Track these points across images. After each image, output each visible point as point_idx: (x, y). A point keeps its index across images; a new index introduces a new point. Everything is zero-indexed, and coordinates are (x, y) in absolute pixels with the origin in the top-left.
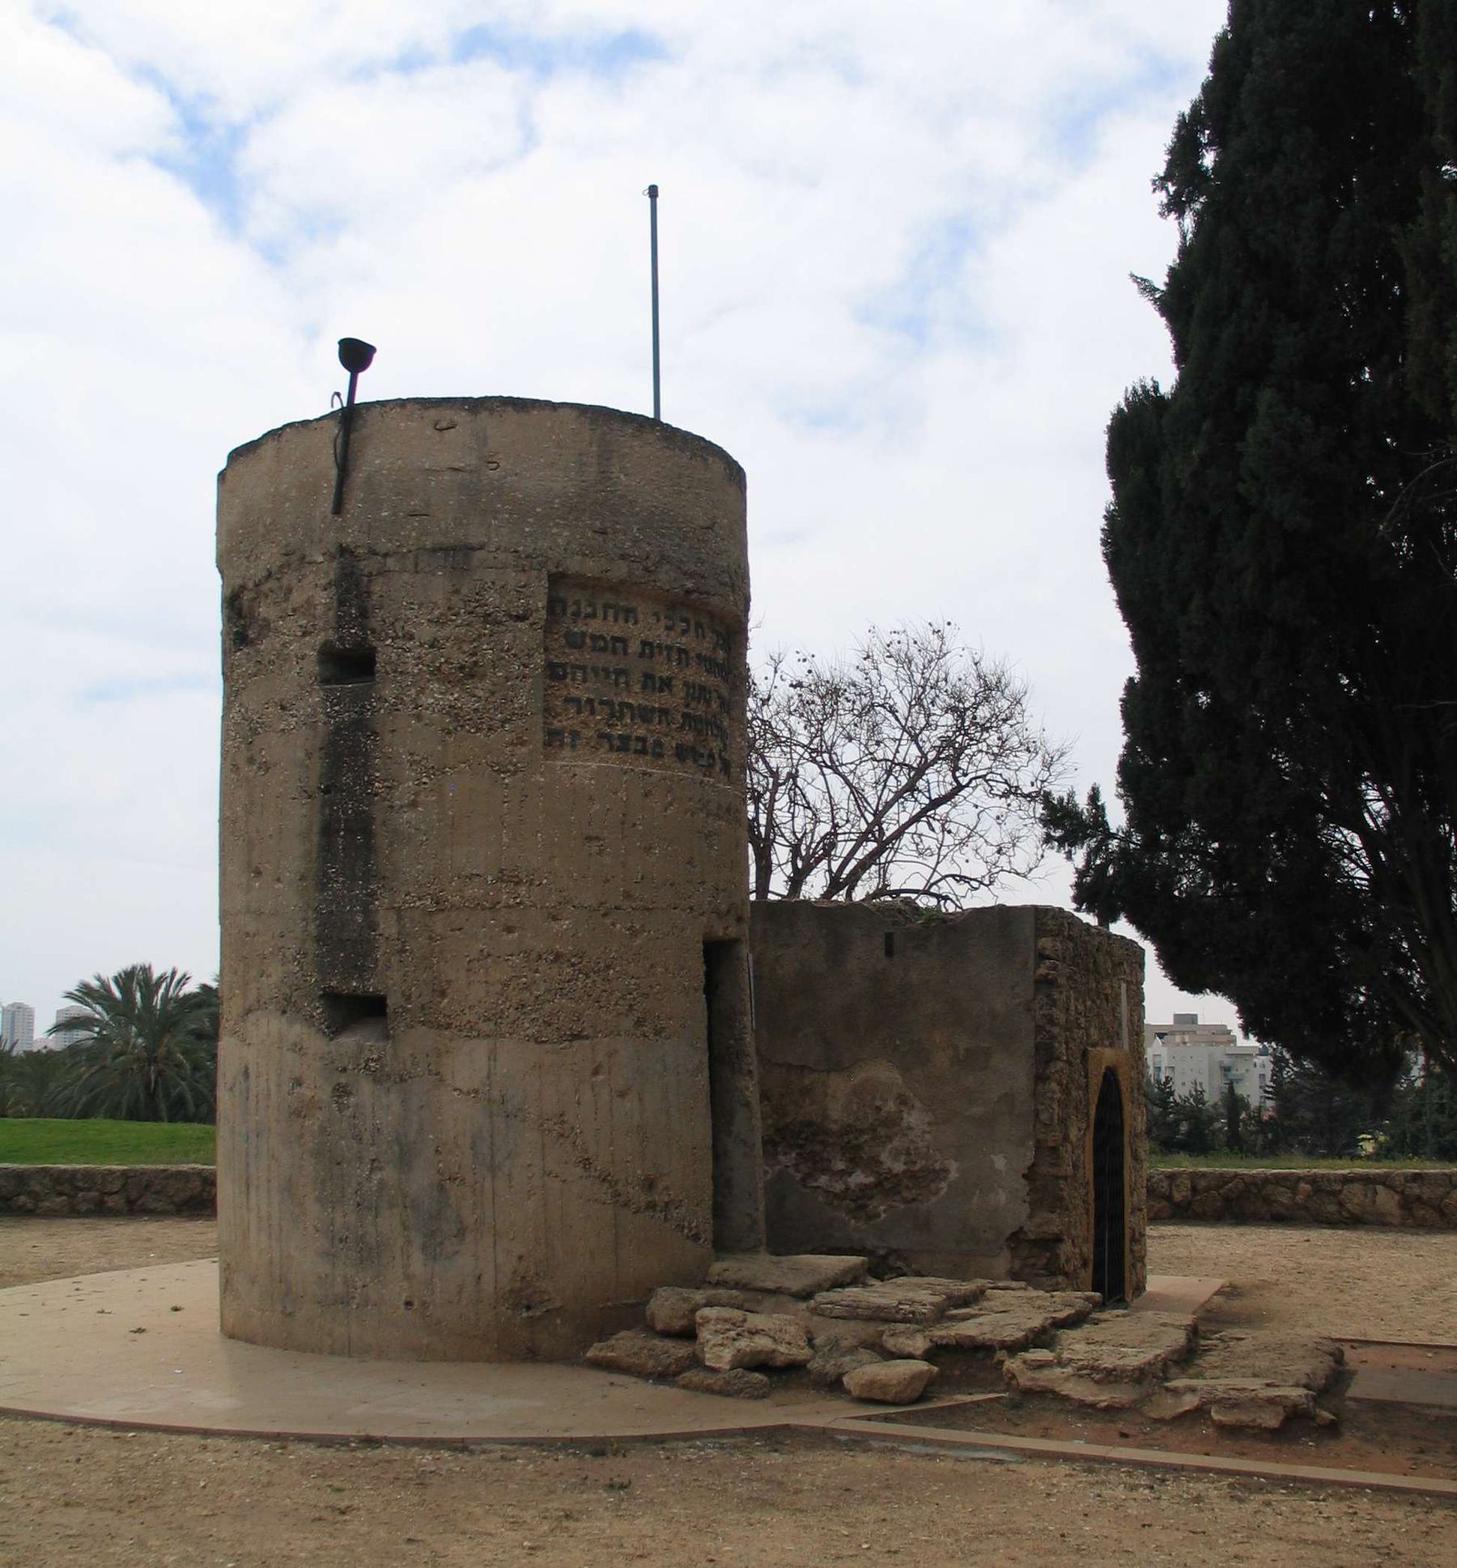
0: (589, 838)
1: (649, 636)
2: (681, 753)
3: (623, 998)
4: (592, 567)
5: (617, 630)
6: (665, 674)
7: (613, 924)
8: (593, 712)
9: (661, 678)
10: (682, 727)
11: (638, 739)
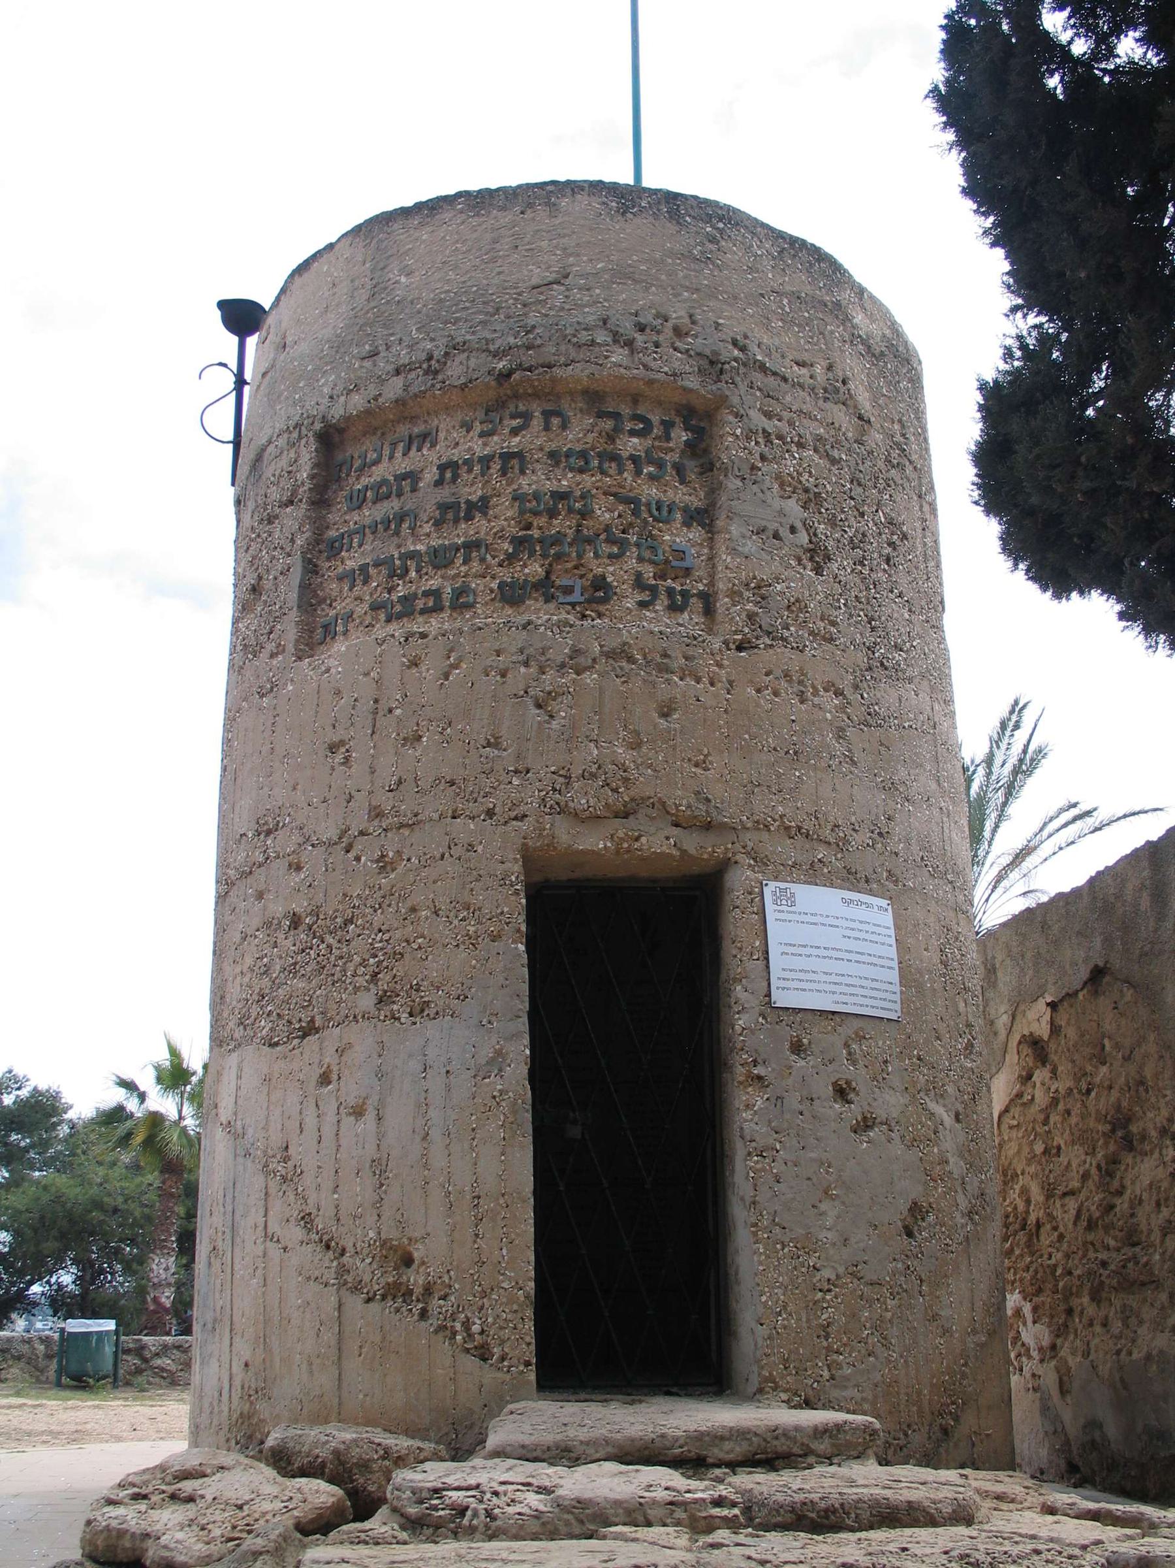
0: (333, 748)
1: (456, 455)
2: (511, 595)
3: (363, 963)
4: (358, 402)
5: (402, 465)
6: (474, 498)
7: (358, 859)
8: (366, 582)
9: (468, 502)
10: (511, 558)
11: (427, 594)
